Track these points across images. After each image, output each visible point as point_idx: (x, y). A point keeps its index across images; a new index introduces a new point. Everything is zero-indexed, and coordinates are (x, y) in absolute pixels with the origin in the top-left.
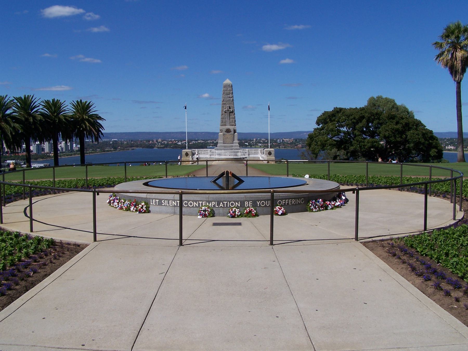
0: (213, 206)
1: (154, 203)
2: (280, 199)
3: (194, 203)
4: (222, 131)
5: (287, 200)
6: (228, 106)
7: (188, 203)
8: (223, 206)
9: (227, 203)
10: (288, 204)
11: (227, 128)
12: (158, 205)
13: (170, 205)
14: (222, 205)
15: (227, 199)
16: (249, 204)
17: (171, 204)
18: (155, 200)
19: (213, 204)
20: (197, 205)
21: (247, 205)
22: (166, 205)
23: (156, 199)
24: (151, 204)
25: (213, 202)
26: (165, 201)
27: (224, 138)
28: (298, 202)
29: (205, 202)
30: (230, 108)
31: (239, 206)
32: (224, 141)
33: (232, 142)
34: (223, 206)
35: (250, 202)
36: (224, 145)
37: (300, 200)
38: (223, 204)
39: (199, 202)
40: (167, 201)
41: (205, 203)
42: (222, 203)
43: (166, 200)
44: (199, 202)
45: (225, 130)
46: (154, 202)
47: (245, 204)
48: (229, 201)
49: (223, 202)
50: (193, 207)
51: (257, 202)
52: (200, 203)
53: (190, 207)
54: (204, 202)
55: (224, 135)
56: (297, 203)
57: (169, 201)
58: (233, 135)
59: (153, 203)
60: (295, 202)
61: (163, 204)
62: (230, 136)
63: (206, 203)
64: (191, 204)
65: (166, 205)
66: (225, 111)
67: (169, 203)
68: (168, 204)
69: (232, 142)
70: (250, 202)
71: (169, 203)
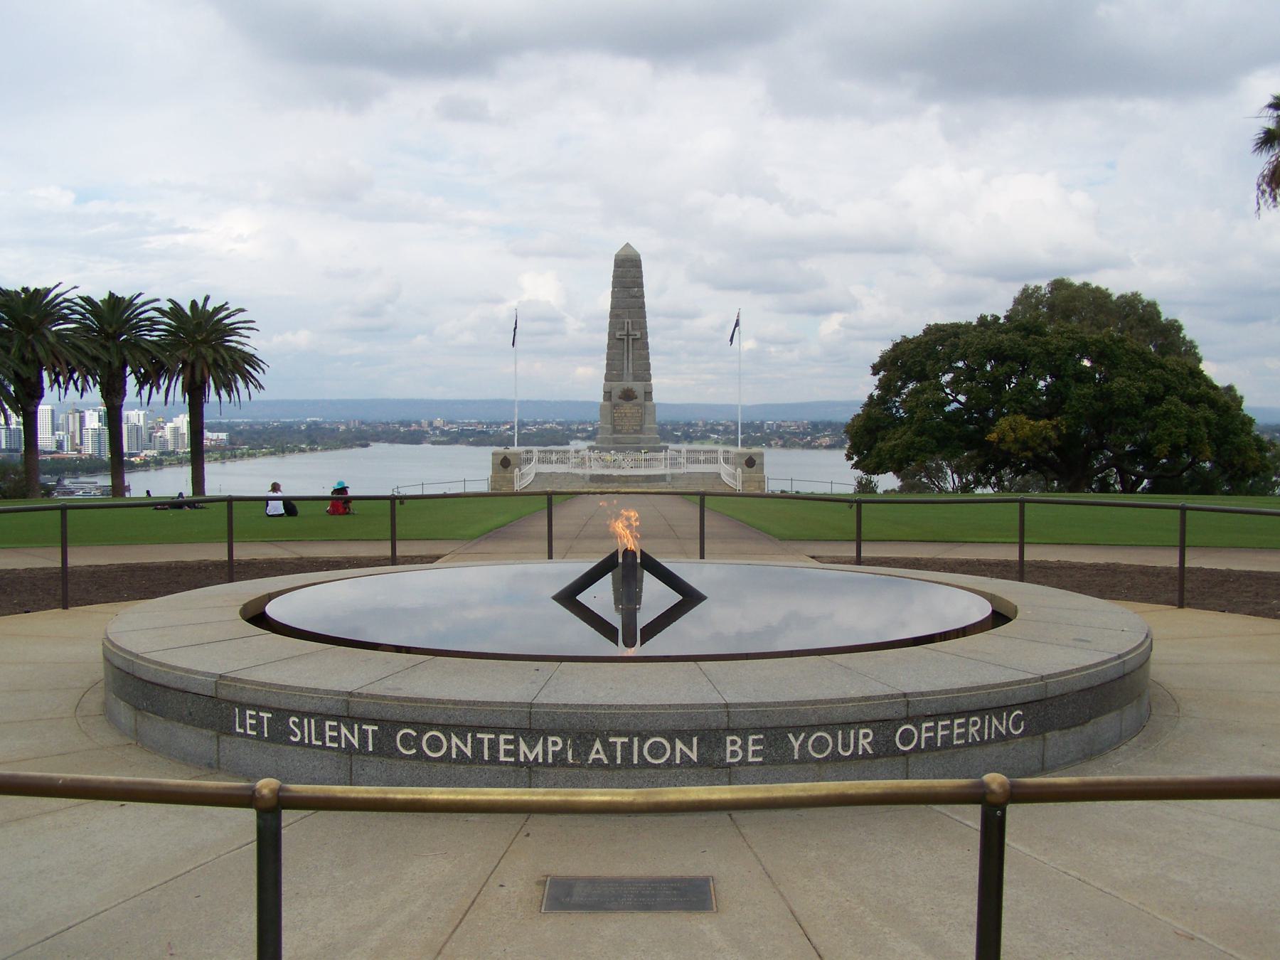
0: (550, 761)
1: (253, 727)
2: (908, 719)
3: (449, 740)
4: (611, 396)
5: (940, 723)
6: (628, 323)
7: (418, 739)
8: (606, 762)
9: (631, 741)
10: (947, 740)
11: (626, 388)
12: (271, 739)
13: (328, 744)
14: (602, 756)
15: (628, 724)
16: (744, 748)
17: (332, 739)
18: (254, 713)
19: (551, 749)
20: (468, 751)
21: (734, 754)
22: (307, 741)
23: (259, 708)
24: (238, 730)
25: (551, 739)
26: (301, 722)
28: (996, 728)
29: (511, 737)
30: (633, 329)
31: (694, 756)
32: (614, 427)
34: (606, 762)
35: (751, 738)
36: (615, 436)
37: (1004, 722)
38: (609, 748)
39: (479, 736)
40: (313, 721)
41: (507, 742)
42: (603, 746)
43: (310, 715)
44: (479, 736)
45: (616, 392)
46: (249, 721)
47: (725, 750)
48: (639, 734)
49: (609, 735)
50: (446, 758)
51: (790, 736)
52: (482, 741)
53: (428, 758)
54: (502, 737)
55: (615, 406)
56: (989, 734)
57: (324, 723)
58: (641, 408)
59: (245, 730)
60: (980, 732)
61: (295, 736)
63: (515, 742)
64: (435, 744)
65: (310, 745)
67: (321, 735)
68: (316, 739)
69: (638, 428)
70: (751, 738)
71: (321, 735)
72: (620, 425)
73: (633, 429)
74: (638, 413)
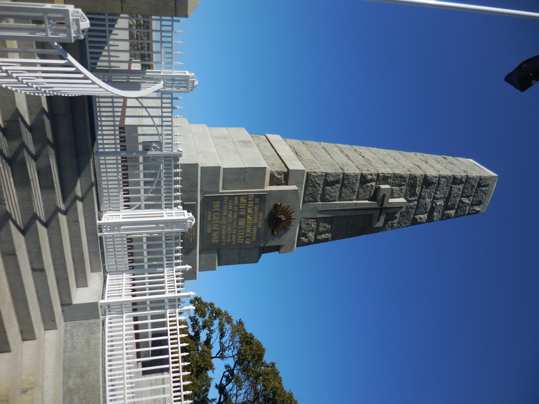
27: (243, 200)
33: (215, 240)
55: (262, 198)
62: (248, 231)
66: (384, 195)
69: (215, 240)
72: (221, 207)
73: (215, 231)
74: (245, 238)
